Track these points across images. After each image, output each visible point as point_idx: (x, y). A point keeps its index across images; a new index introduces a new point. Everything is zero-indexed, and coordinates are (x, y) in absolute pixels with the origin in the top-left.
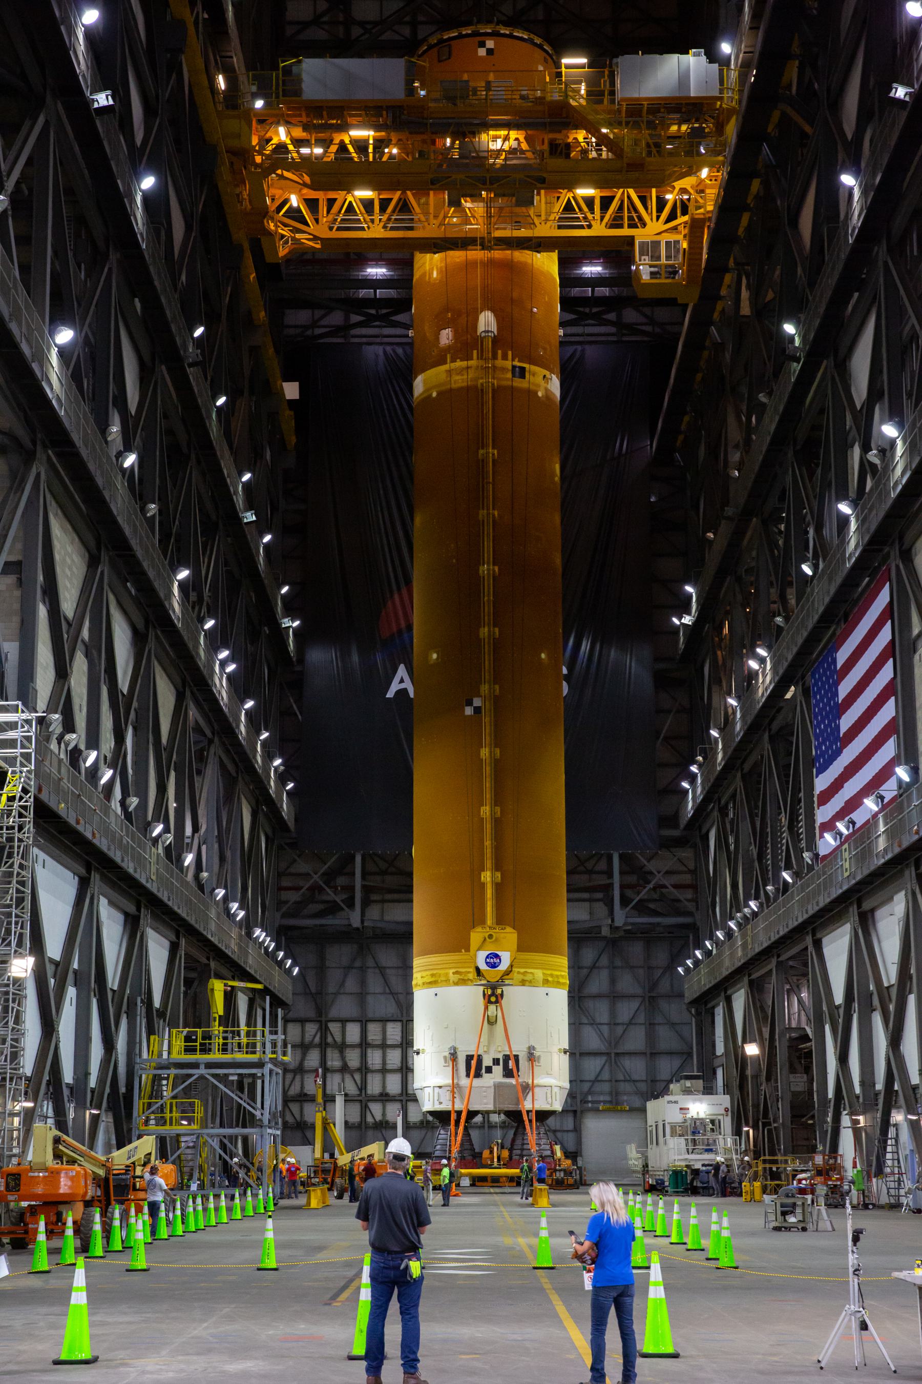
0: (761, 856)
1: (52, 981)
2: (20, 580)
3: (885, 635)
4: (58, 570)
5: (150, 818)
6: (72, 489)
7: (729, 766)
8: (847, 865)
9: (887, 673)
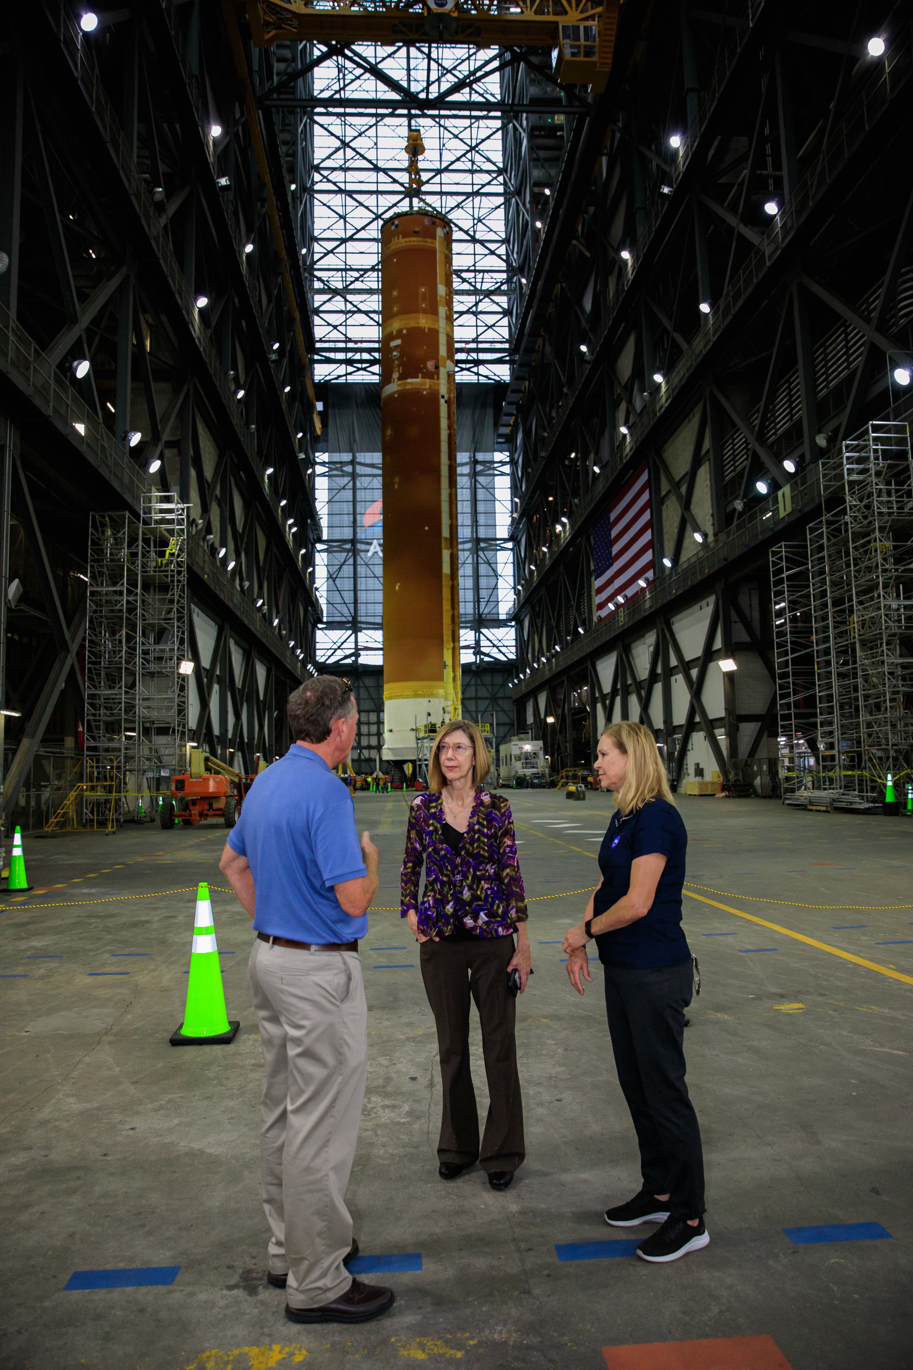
0: (557, 626)
1: (205, 680)
2: (179, 451)
3: (646, 496)
4: (202, 452)
5: (255, 596)
6: (207, 404)
7: (540, 583)
8: (622, 619)
9: (646, 516)
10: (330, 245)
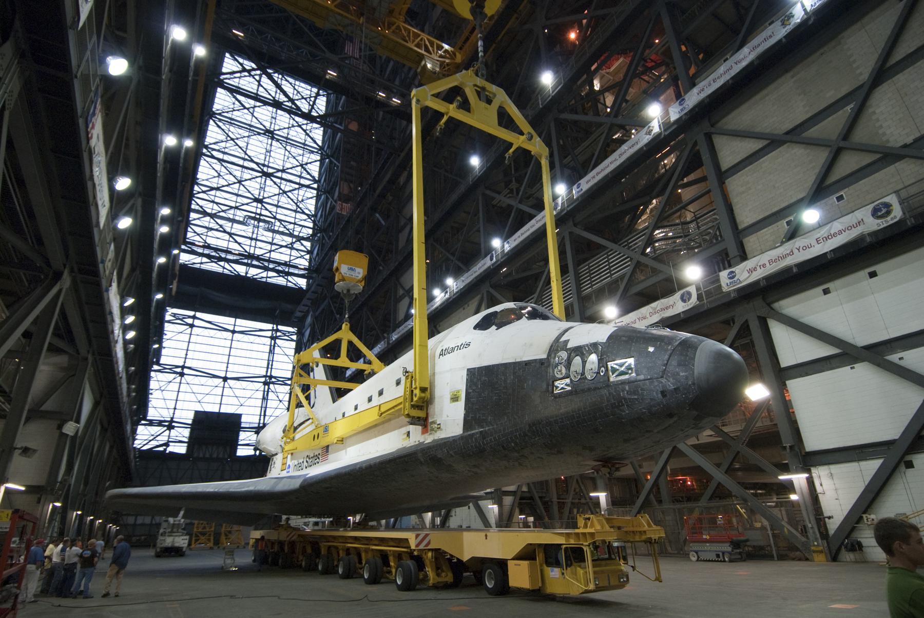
10: (204, 189)
